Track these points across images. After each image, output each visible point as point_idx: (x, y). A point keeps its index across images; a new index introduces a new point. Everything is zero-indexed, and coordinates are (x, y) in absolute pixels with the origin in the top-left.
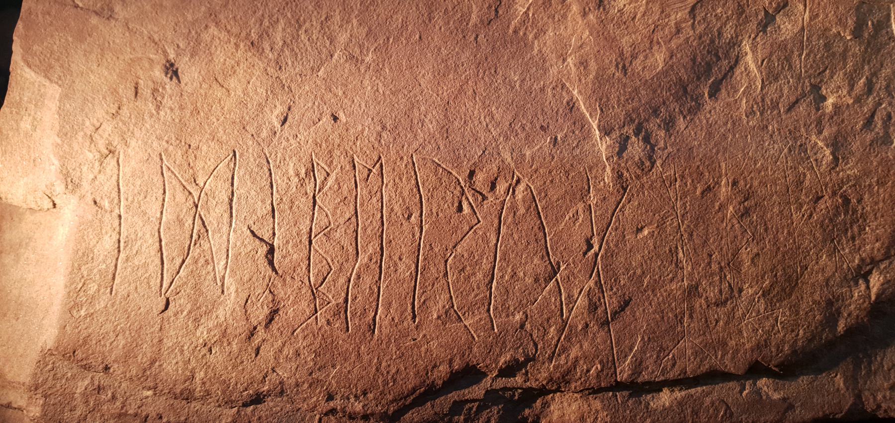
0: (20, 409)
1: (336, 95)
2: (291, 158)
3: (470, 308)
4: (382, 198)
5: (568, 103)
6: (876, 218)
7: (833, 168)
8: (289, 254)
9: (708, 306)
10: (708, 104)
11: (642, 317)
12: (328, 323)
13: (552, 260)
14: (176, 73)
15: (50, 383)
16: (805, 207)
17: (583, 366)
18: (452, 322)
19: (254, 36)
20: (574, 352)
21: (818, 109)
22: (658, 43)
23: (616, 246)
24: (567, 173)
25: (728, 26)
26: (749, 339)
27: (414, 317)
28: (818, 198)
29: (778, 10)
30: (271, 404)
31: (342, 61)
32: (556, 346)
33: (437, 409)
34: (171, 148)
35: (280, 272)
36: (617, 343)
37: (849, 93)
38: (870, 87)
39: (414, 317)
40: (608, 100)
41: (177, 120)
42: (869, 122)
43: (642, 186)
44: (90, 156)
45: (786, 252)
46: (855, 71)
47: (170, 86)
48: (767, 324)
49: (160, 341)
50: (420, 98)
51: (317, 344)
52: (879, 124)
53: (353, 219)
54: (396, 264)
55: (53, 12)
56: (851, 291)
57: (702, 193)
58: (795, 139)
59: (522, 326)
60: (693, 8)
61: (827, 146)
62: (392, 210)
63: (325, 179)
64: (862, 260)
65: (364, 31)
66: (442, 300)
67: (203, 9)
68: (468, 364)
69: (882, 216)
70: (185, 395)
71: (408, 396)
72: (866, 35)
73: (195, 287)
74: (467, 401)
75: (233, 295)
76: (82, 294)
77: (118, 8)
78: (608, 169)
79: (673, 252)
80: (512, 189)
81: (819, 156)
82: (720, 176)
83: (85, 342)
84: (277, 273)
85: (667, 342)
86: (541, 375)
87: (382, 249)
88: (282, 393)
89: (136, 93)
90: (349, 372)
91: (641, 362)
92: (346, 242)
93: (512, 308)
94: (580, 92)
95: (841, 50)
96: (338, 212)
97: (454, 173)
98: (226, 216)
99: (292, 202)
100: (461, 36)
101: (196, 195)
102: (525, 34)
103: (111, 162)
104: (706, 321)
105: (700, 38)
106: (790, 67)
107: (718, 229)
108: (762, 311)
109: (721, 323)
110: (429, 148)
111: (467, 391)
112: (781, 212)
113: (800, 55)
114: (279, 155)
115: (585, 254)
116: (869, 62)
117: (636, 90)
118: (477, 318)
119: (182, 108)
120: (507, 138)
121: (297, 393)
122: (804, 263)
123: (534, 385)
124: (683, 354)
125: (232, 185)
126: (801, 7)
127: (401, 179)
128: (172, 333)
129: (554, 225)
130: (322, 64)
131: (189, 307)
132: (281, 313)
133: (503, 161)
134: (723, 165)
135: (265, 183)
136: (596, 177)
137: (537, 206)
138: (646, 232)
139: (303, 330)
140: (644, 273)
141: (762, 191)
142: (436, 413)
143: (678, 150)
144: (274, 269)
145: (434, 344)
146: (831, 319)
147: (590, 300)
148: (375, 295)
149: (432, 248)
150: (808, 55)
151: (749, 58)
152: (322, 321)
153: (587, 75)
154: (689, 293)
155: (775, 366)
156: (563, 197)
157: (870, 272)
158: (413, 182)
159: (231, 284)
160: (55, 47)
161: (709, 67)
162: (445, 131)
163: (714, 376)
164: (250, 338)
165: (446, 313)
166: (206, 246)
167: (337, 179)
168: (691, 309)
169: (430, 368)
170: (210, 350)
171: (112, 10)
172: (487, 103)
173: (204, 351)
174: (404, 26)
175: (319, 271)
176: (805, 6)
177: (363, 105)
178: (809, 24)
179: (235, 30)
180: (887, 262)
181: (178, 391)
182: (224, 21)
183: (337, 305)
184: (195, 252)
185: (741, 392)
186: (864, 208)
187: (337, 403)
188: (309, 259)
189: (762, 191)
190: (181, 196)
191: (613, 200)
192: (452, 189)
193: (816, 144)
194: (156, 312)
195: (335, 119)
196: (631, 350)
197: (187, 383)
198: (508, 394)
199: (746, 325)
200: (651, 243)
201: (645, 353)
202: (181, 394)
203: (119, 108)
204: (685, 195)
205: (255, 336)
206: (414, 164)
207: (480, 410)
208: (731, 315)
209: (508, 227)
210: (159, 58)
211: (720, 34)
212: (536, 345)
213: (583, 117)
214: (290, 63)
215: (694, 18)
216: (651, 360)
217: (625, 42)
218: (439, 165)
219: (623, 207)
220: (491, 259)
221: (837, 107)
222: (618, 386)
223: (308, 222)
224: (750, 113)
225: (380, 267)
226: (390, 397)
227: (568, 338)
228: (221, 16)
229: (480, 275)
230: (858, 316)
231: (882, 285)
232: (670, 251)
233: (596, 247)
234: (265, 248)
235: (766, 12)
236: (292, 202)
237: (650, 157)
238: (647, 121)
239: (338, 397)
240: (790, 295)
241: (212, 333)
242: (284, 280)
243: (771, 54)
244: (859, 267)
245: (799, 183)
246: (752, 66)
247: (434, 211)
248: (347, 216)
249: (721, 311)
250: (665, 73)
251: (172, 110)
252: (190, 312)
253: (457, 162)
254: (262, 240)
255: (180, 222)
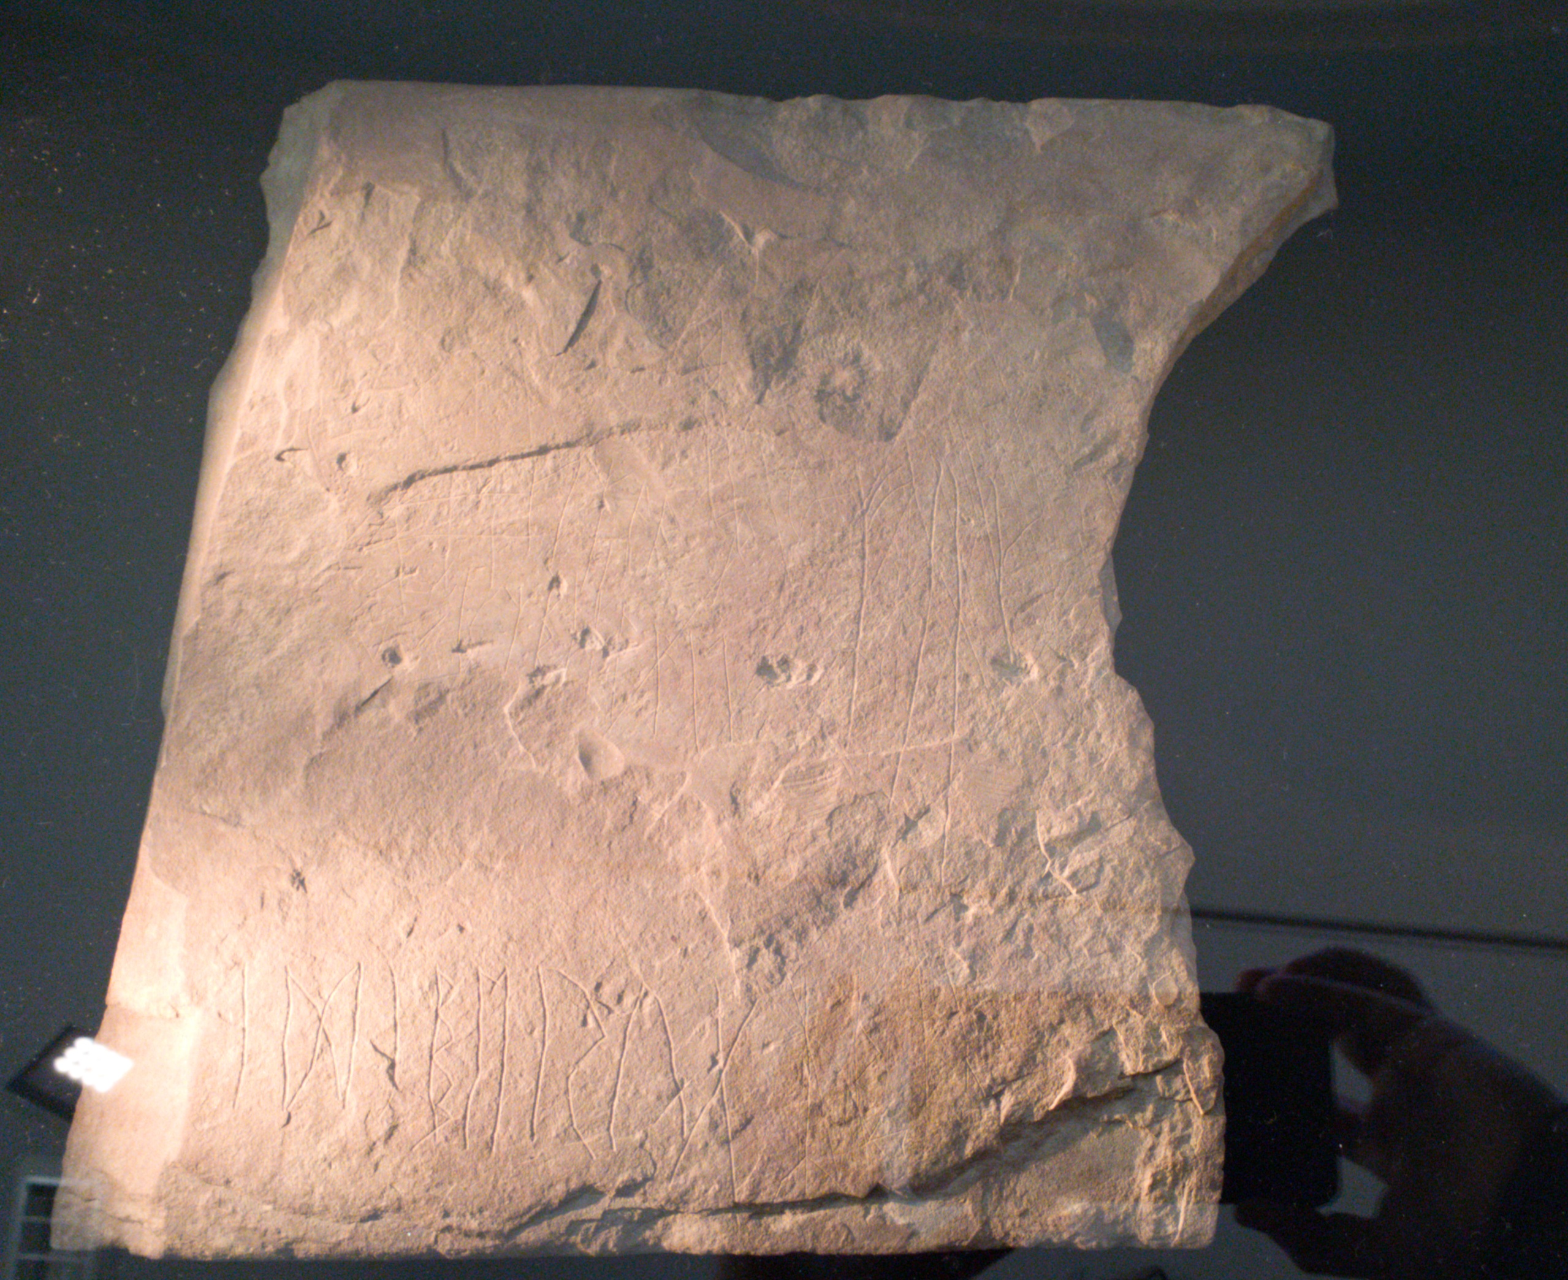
0: (140, 1222)
1: (463, 905)
2: (415, 970)
3: (590, 1127)
4: (505, 1012)
5: (700, 913)
6: (1011, 1036)
7: (970, 982)
8: (409, 1070)
9: (831, 1125)
10: (844, 914)
11: (765, 1134)
12: (447, 1139)
13: (676, 1077)
14: (302, 882)
15: (172, 1196)
16: (938, 1023)
17: (701, 1186)
18: (571, 1140)
19: (383, 844)
20: (693, 1172)
21: (957, 920)
22: (793, 852)
23: (741, 1061)
24: (696, 986)
25: (866, 834)
26: (871, 1161)
27: (532, 1135)
28: (952, 1014)
29: (920, 815)
30: (389, 1220)
31: (471, 869)
32: (675, 1165)
33: (554, 1229)
34: (297, 961)
35: (400, 1087)
36: (737, 1162)
37: (990, 903)
38: (1012, 897)
39: (532, 1135)
40: (739, 910)
41: (303, 932)
42: (1009, 934)
43: (771, 1000)
44: (215, 967)
45: (915, 1071)
46: (997, 880)
47: (296, 895)
48: (891, 1146)
49: (281, 1155)
50: (549, 907)
51: (434, 1161)
52: (1021, 936)
53: (475, 1034)
54: (516, 1081)
55: (181, 819)
56: (980, 1113)
57: (833, 1007)
58: (932, 951)
59: (642, 1145)
60: (831, 815)
61: (965, 959)
62: (515, 1024)
63: (449, 992)
64: (993, 1080)
65: (494, 838)
66: (561, 1118)
67: (331, 816)
68: (584, 1184)
69: (1018, 1034)
70: (304, 1210)
71: (524, 1214)
72: (1009, 843)
73: (319, 1102)
74: (584, 1221)
75: (354, 1110)
76: (205, 1106)
77: (245, 815)
78: (738, 982)
79: (798, 1069)
80: (639, 1002)
81: (957, 969)
82: (852, 990)
83: (208, 1155)
84: (397, 1088)
85: (787, 1163)
86: (658, 1195)
87: (502, 1065)
88: (399, 1209)
89: (262, 904)
90: (466, 1189)
91: (760, 1183)
92: (468, 1057)
93: (632, 1127)
94: (712, 902)
95: (983, 858)
96: (460, 1026)
97: (580, 985)
98: (349, 1030)
99: (414, 1016)
100: (594, 843)
101: (320, 1008)
102: (659, 841)
103: (236, 975)
104: (828, 1141)
105: (836, 846)
106: (930, 875)
107: (845, 1045)
108: (887, 1131)
109: (844, 1144)
110: (555, 959)
111: (584, 1211)
112: (913, 1028)
113: (940, 864)
114: (404, 967)
115: (710, 1070)
116: (1011, 871)
117: (768, 901)
118: (596, 1137)
119: (308, 919)
120: (637, 949)
121: (414, 1209)
122: (933, 1082)
123: (653, 1205)
124: (802, 1175)
125: (356, 998)
126: (943, 813)
127: (525, 992)
128: (293, 1147)
129: (681, 1040)
130: (451, 872)
131: (310, 1122)
132: (400, 1128)
133: (631, 973)
134: (855, 978)
135: (390, 997)
136: (725, 990)
137: (663, 1020)
138: (772, 1048)
139: (421, 1147)
140: (767, 1090)
141: (894, 1006)
142: (552, 1233)
143: (810, 962)
144: (394, 1084)
145: (551, 1163)
146: (957, 1142)
147: (711, 1119)
148: (494, 1113)
149: (553, 1064)
150: (948, 863)
151: (888, 866)
152: (440, 1138)
153: (719, 885)
154: (812, 1111)
155: (899, 1190)
156: (691, 1011)
157: (1001, 1093)
158: (538, 995)
159: (353, 1098)
160: (183, 856)
161: (844, 879)
162: (573, 942)
163: (831, 1199)
164: (369, 1153)
165: (565, 1131)
166: (328, 1060)
167: (460, 993)
168: (814, 1129)
169: (546, 1187)
170: (330, 1165)
171: (239, 816)
172: (618, 911)
173: (324, 1165)
174: (536, 832)
175: (439, 1087)
176: (947, 812)
177: (490, 914)
178: (950, 832)
179: (364, 838)
180: (1019, 1083)
181: (297, 1206)
182: (352, 829)
183: (456, 1122)
184: (318, 1066)
185: (865, 1217)
186: (999, 1025)
187: (453, 1220)
188: (429, 1074)
189: (894, 1006)
190: (305, 1010)
191: (740, 1015)
192: (577, 1001)
193: (954, 956)
194: (277, 1126)
195: (461, 929)
196: (750, 1169)
197: (307, 1198)
198: (627, 1215)
199: (869, 1146)
200: (776, 1059)
201: (763, 1173)
202: (300, 1208)
203: (245, 919)
204: (813, 1009)
205: (375, 1152)
206: (539, 976)
207: (598, 1230)
208: (854, 1136)
209: (633, 1043)
210: (286, 868)
211: (858, 841)
212: (655, 1164)
213: (715, 927)
214: (418, 872)
215: (831, 825)
216: (770, 1181)
217: (759, 852)
218: (565, 977)
219: (751, 1021)
220: (614, 1075)
221: (978, 920)
222: (736, 1207)
223: (429, 1037)
224: (887, 923)
225: (500, 1083)
226: (506, 1215)
227: (688, 1158)
228: (350, 824)
229: (602, 1093)
230: (986, 1139)
231: (1013, 1106)
232: (795, 1067)
233: (721, 1063)
234: (386, 1064)
235: (907, 818)
236: (414, 1016)
237: (780, 970)
238: (779, 932)
239: (455, 1213)
240: (917, 1115)
241: (332, 1148)
242: (404, 1096)
243: (910, 862)
244: (990, 1088)
245: (933, 996)
246: (891, 875)
247: (558, 1025)
248: (469, 1030)
249: (845, 1131)
250: (798, 882)
251: (298, 921)
252: (311, 1127)
253: (583, 973)
254: (383, 1055)
255: (303, 1035)
